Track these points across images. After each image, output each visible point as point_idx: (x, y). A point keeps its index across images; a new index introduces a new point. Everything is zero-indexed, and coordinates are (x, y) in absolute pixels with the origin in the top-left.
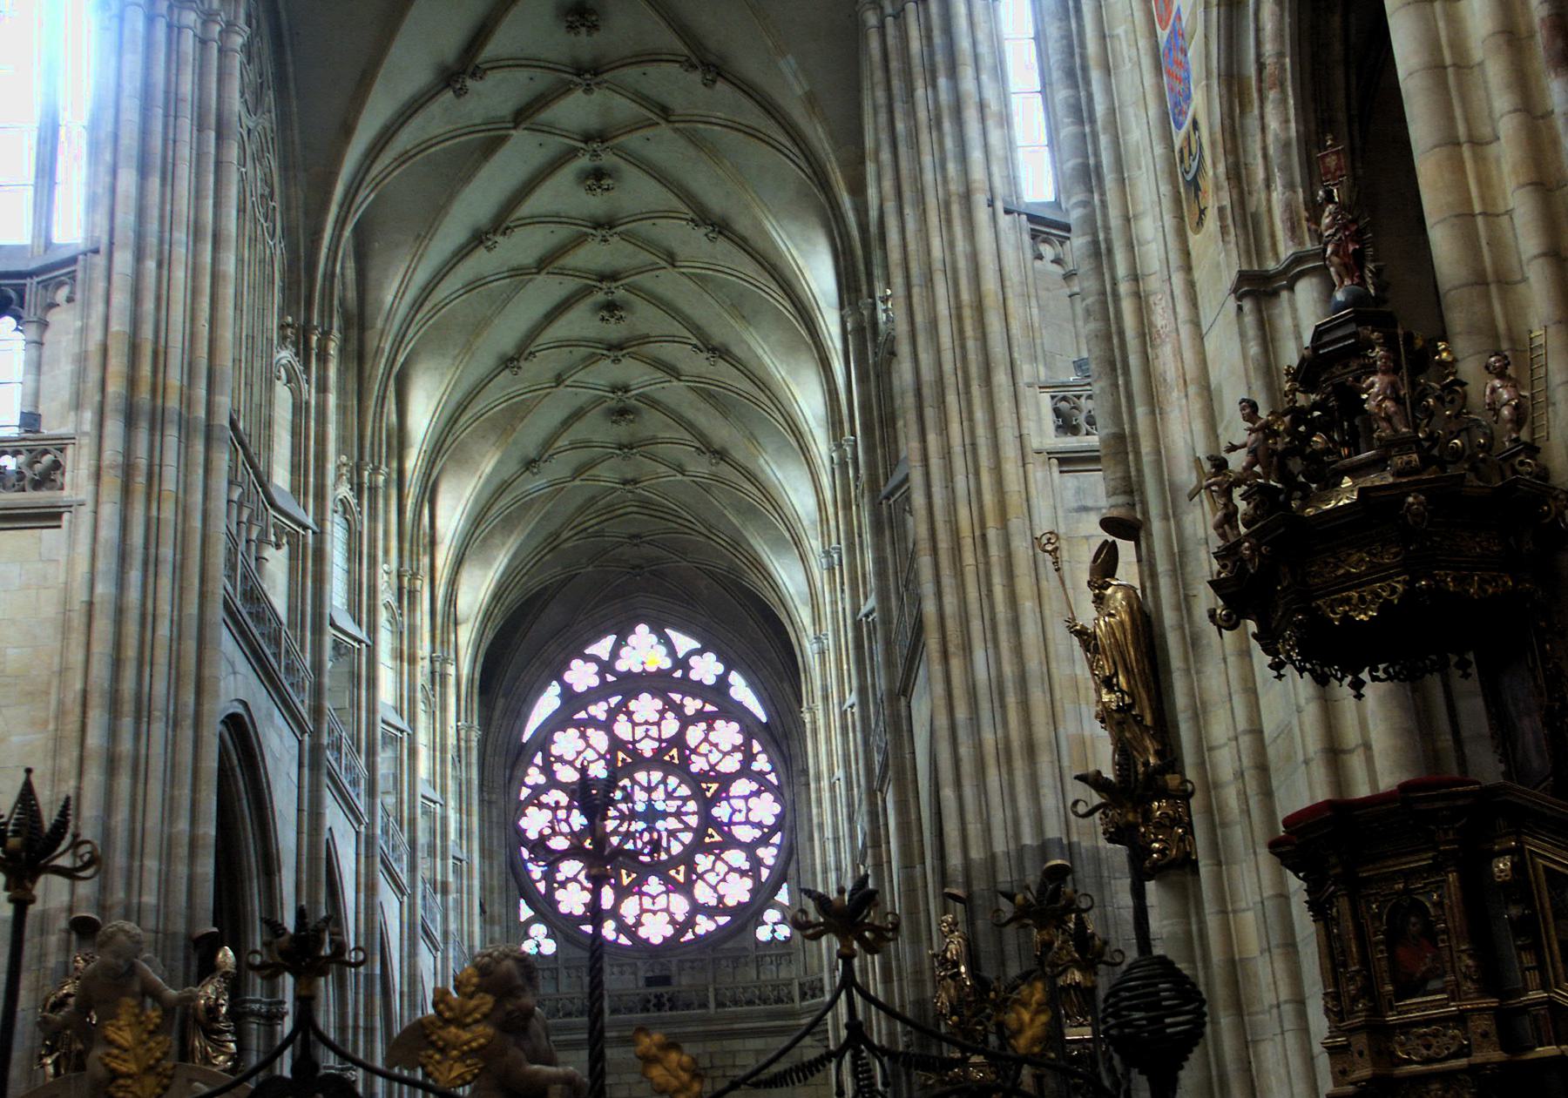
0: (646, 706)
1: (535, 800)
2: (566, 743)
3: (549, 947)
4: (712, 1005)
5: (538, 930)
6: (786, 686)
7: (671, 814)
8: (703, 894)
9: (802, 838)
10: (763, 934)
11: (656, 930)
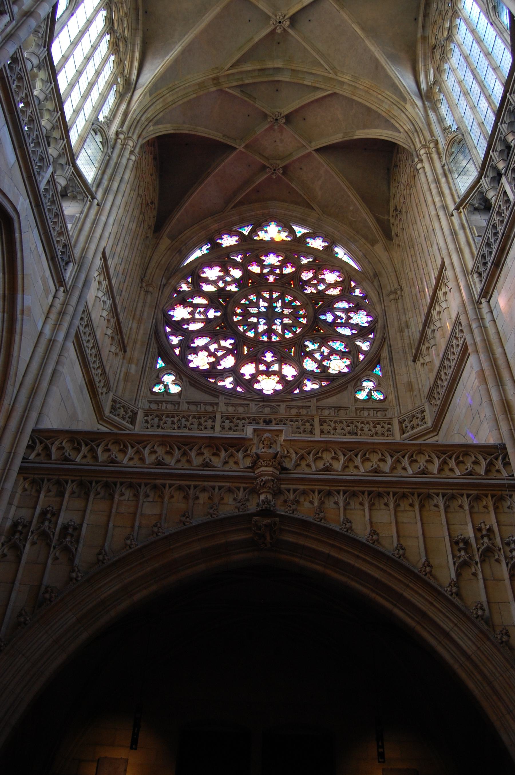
0: (272, 260)
1: (183, 300)
2: (212, 273)
3: (175, 389)
4: (317, 431)
5: (169, 379)
6: (379, 248)
7: (286, 316)
8: (310, 365)
9: (392, 331)
10: (362, 396)
11: (268, 385)
